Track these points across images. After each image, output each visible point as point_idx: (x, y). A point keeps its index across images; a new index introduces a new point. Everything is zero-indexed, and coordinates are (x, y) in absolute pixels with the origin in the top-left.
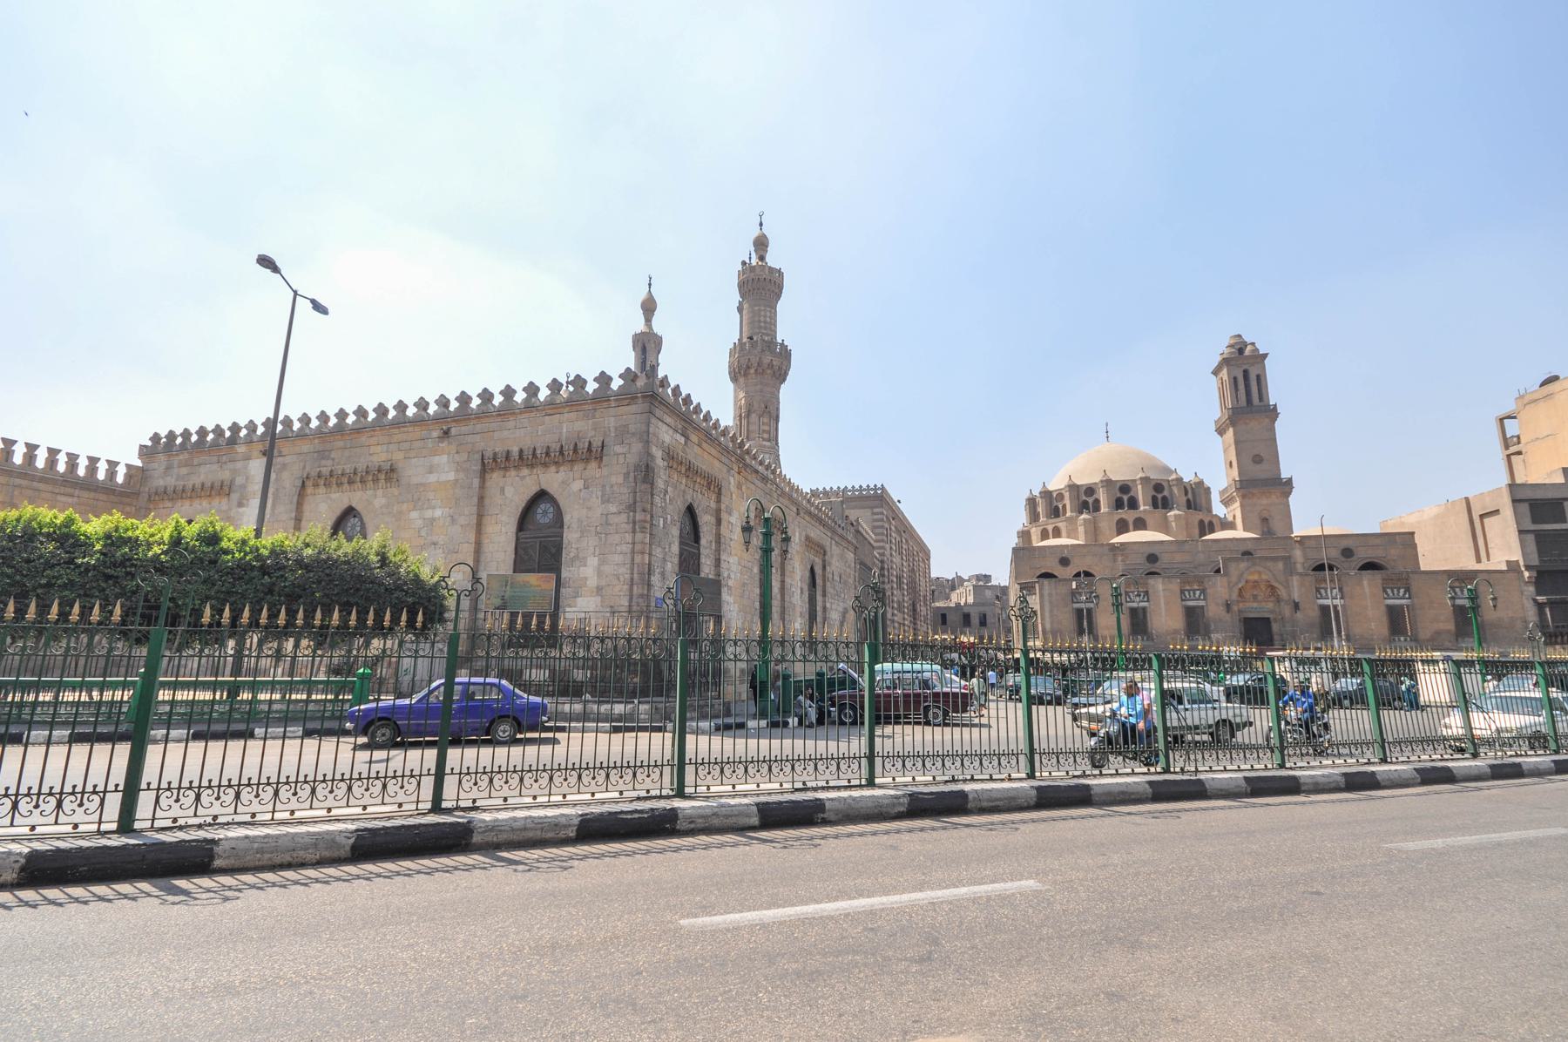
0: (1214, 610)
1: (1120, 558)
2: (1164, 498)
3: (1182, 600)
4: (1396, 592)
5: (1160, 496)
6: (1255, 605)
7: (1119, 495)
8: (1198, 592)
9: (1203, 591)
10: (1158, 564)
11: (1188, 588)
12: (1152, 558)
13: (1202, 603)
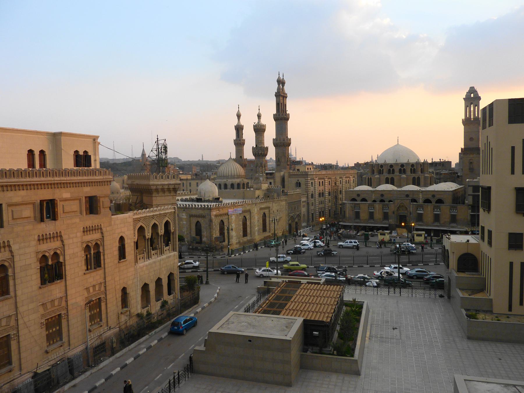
0: (390, 214)
1: (373, 195)
2: (404, 169)
3: (383, 210)
4: (437, 210)
5: (402, 169)
6: (403, 212)
7: (389, 168)
8: (387, 208)
9: (388, 208)
10: (384, 197)
11: (384, 207)
12: (382, 195)
13: (388, 211)
